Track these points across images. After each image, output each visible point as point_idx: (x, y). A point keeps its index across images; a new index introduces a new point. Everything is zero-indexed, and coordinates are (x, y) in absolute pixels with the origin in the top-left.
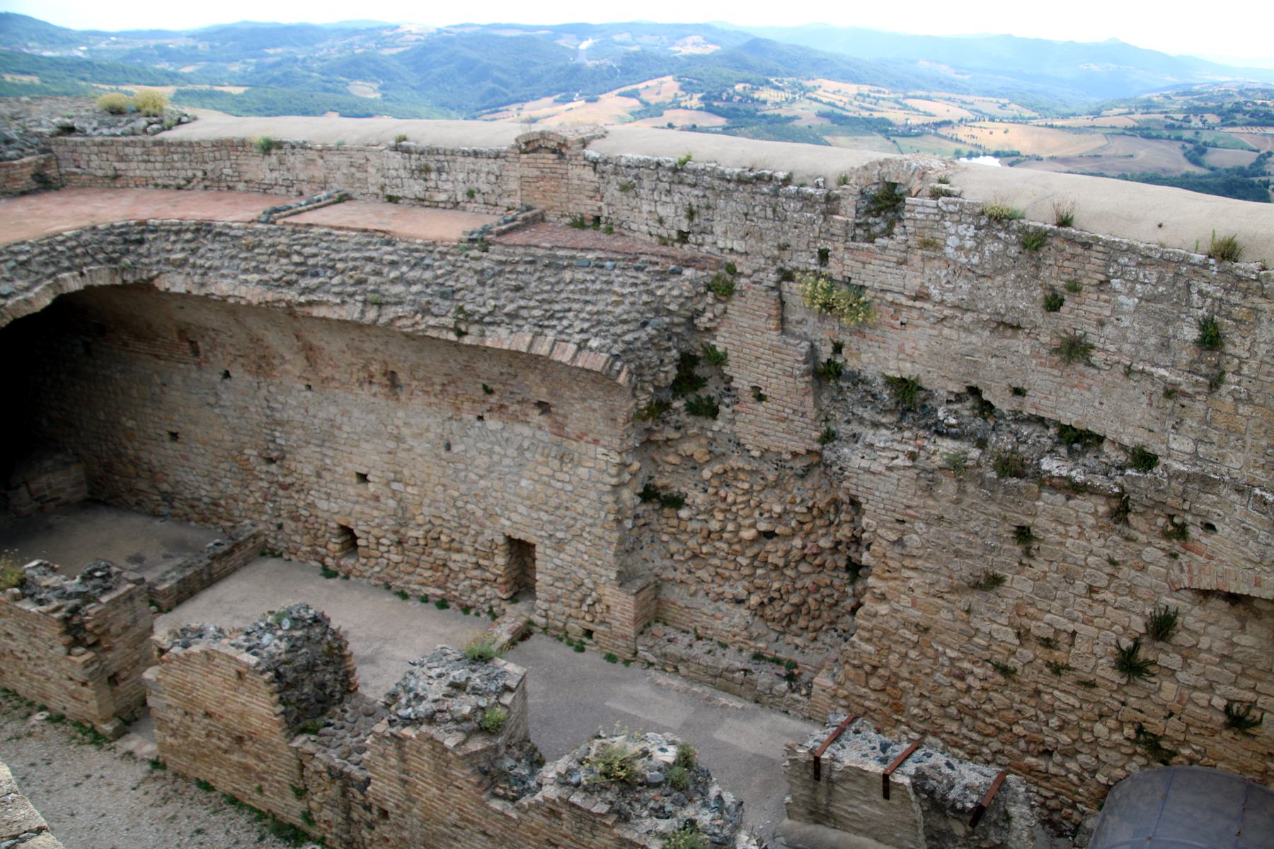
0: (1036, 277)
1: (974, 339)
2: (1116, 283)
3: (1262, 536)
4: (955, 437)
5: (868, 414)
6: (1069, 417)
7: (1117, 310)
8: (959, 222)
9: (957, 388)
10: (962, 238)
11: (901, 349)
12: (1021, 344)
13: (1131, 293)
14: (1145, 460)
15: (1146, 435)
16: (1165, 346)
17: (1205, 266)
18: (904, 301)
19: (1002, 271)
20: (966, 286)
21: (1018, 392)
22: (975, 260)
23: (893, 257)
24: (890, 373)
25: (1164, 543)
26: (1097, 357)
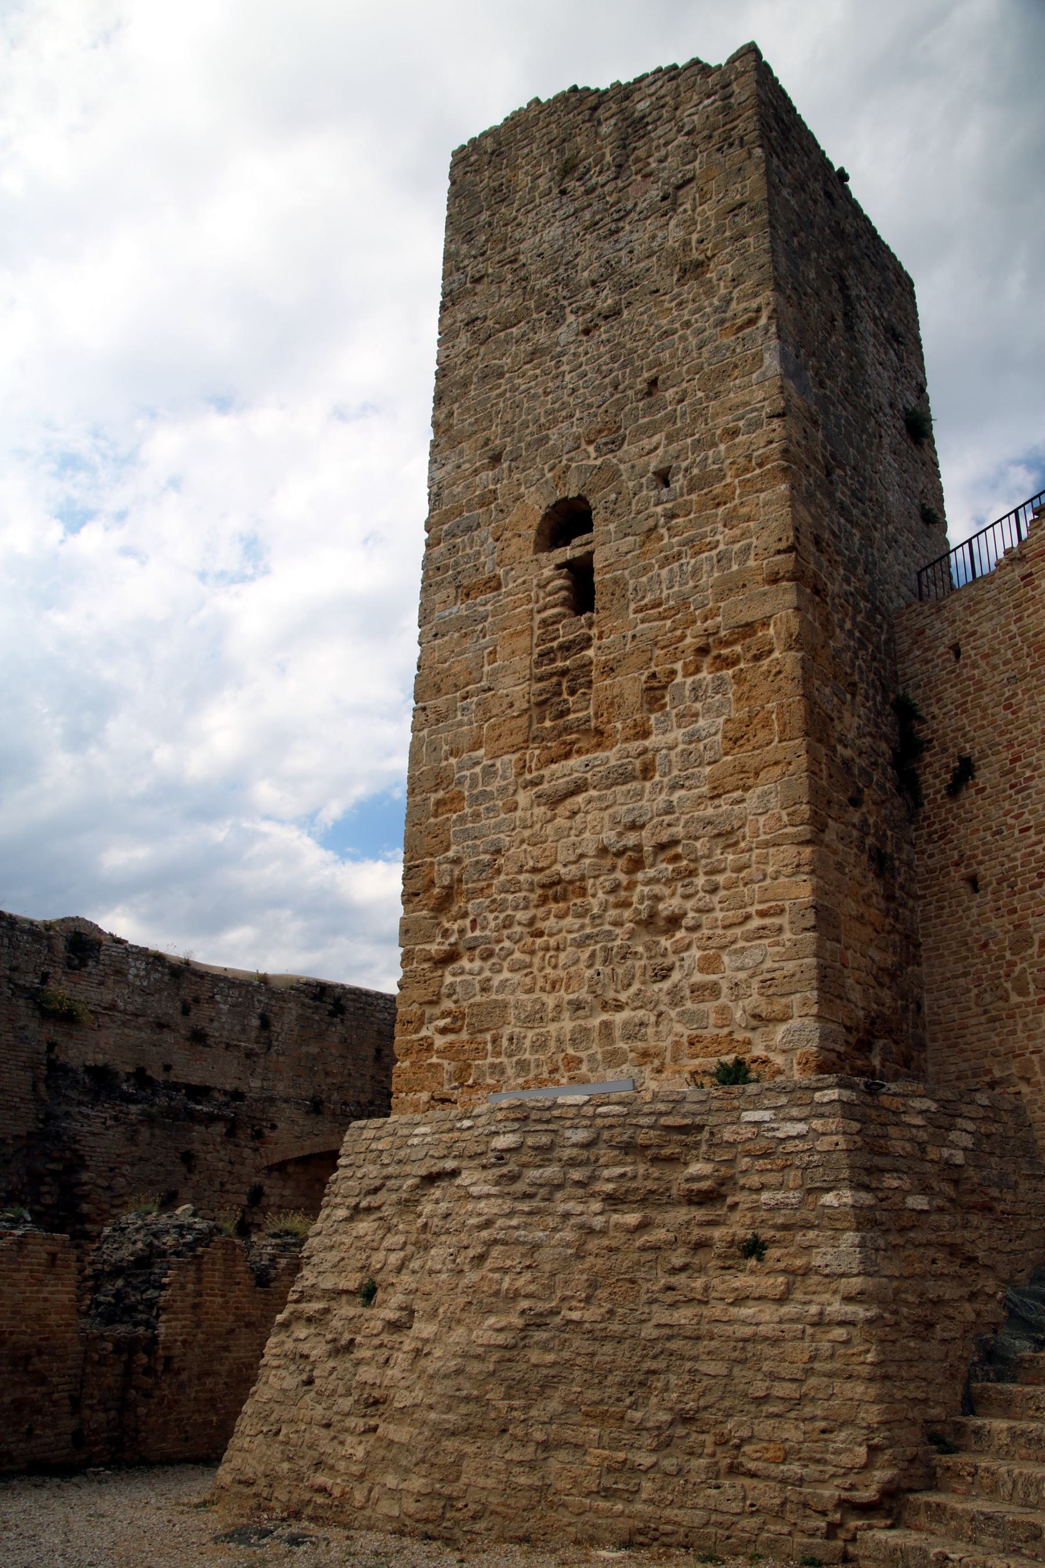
0: (177, 995)
1: (143, 1035)
2: (218, 997)
3: (301, 1122)
4: (136, 1102)
5: (73, 1094)
6: (195, 1080)
7: (219, 1012)
8: (137, 959)
9: (131, 1069)
10: (138, 969)
11: (97, 1044)
12: (168, 1037)
13: (225, 1003)
14: (237, 1095)
15: (237, 1082)
16: (243, 1030)
17: (259, 987)
18: (100, 1010)
19: (160, 991)
20: (139, 1000)
21: (167, 1068)
22: (145, 984)
23: (96, 979)
24: (88, 1063)
25: (252, 1144)
26: (210, 1041)
